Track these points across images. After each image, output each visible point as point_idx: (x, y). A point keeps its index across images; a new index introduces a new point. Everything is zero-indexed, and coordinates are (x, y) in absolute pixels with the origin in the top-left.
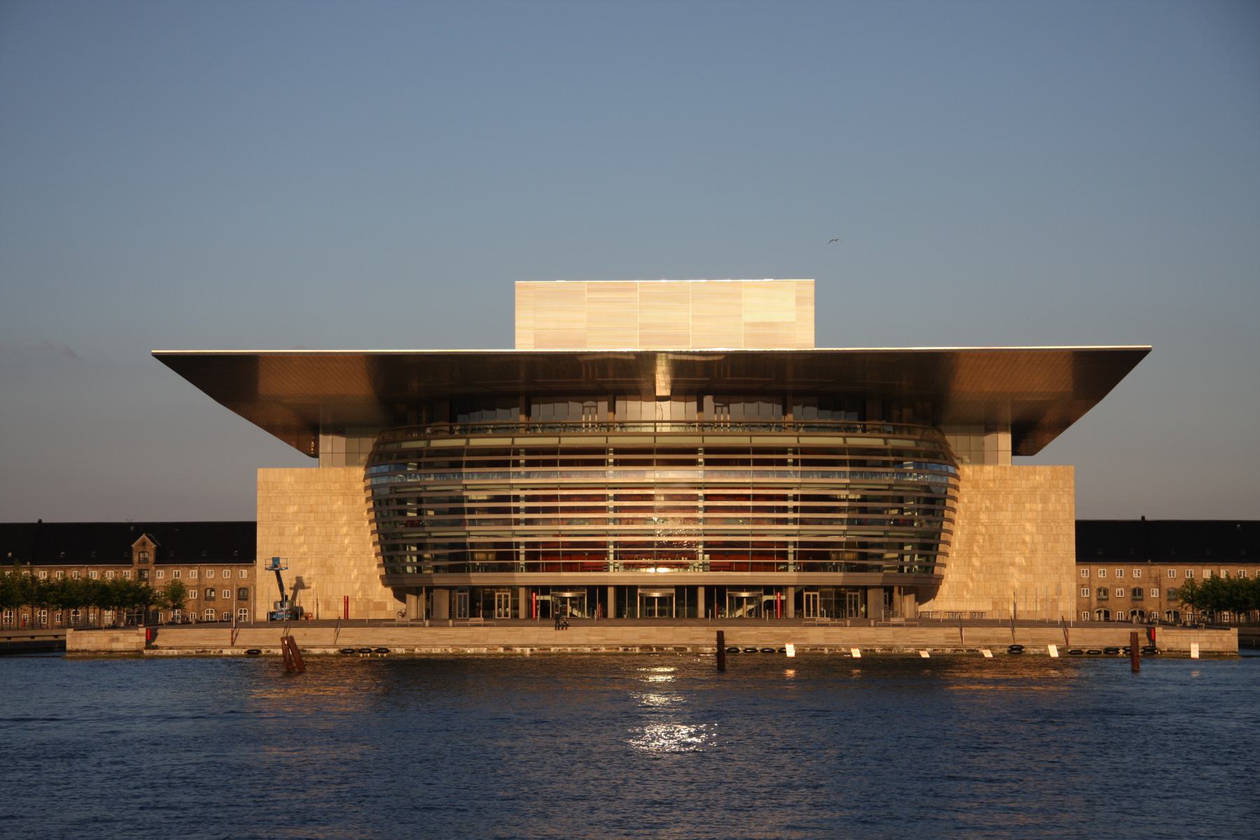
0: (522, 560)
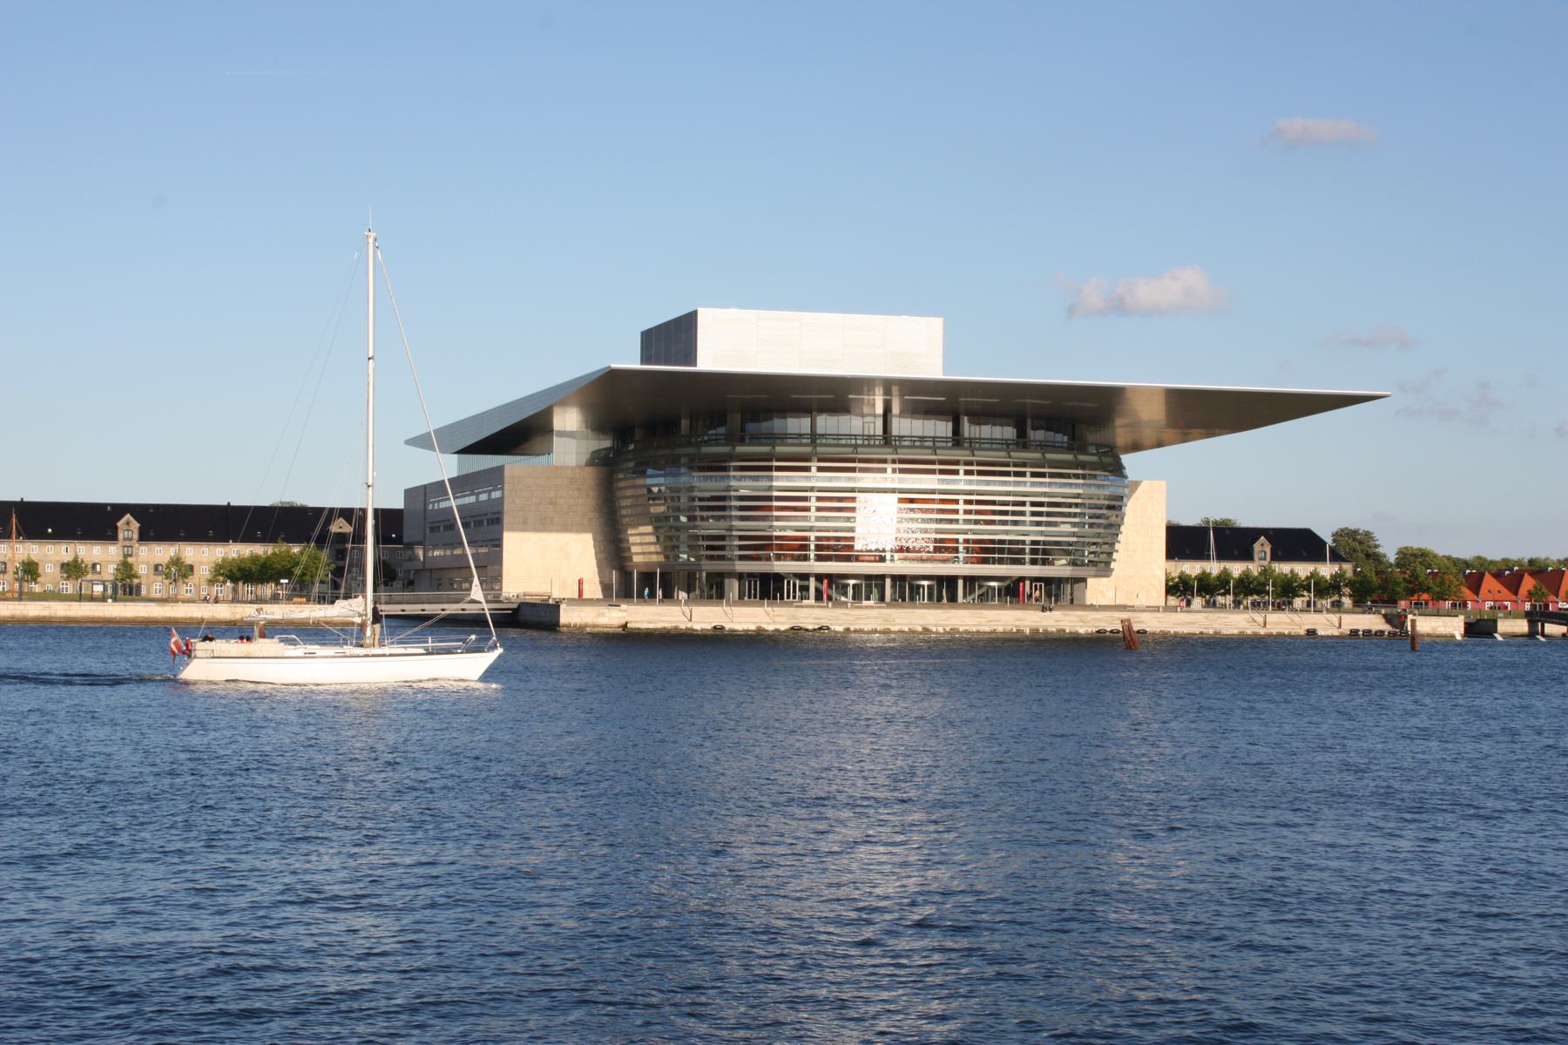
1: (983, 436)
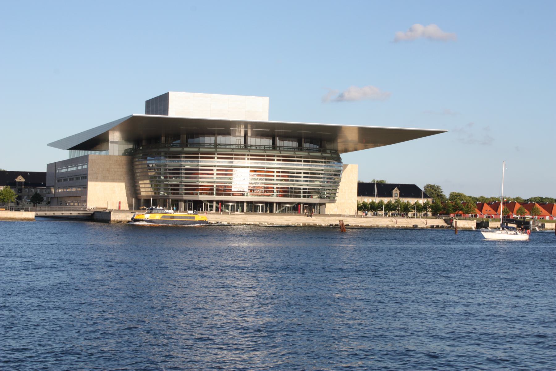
1: (284, 145)
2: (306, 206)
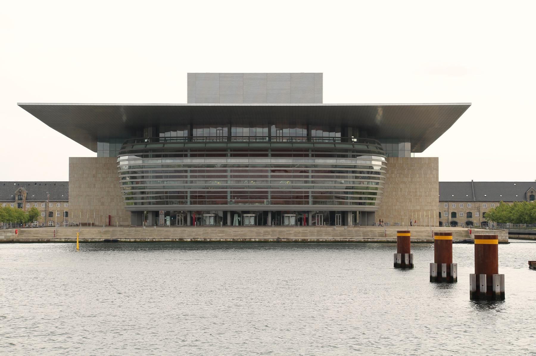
0: (189, 200)
2: (319, 215)
